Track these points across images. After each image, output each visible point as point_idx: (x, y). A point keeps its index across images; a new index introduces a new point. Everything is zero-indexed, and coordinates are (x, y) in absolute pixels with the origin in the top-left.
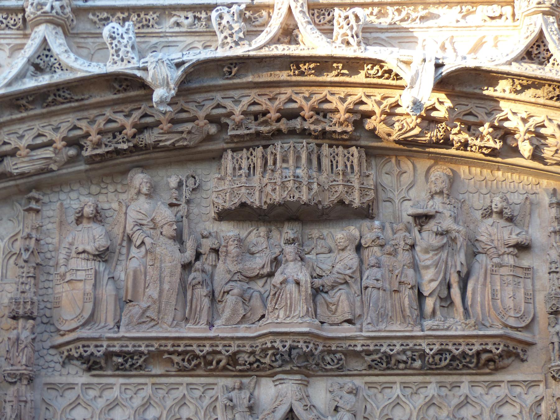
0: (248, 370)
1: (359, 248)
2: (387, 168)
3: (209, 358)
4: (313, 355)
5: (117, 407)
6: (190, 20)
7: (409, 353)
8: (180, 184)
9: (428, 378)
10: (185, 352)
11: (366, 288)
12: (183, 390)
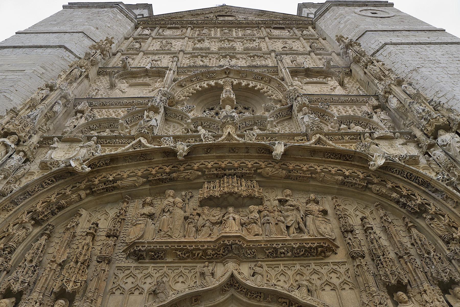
0: (212, 258)
1: (260, 212)
2: (267, 191)
3: (194, 252)
4: (242, 248)
5: (149, 277)
6: (194, 140)
7: (285, 248)
8: (186, 196)
9: (294, 262)
10: (184, 249)
11: (263, 224)
12: (182, 269)
